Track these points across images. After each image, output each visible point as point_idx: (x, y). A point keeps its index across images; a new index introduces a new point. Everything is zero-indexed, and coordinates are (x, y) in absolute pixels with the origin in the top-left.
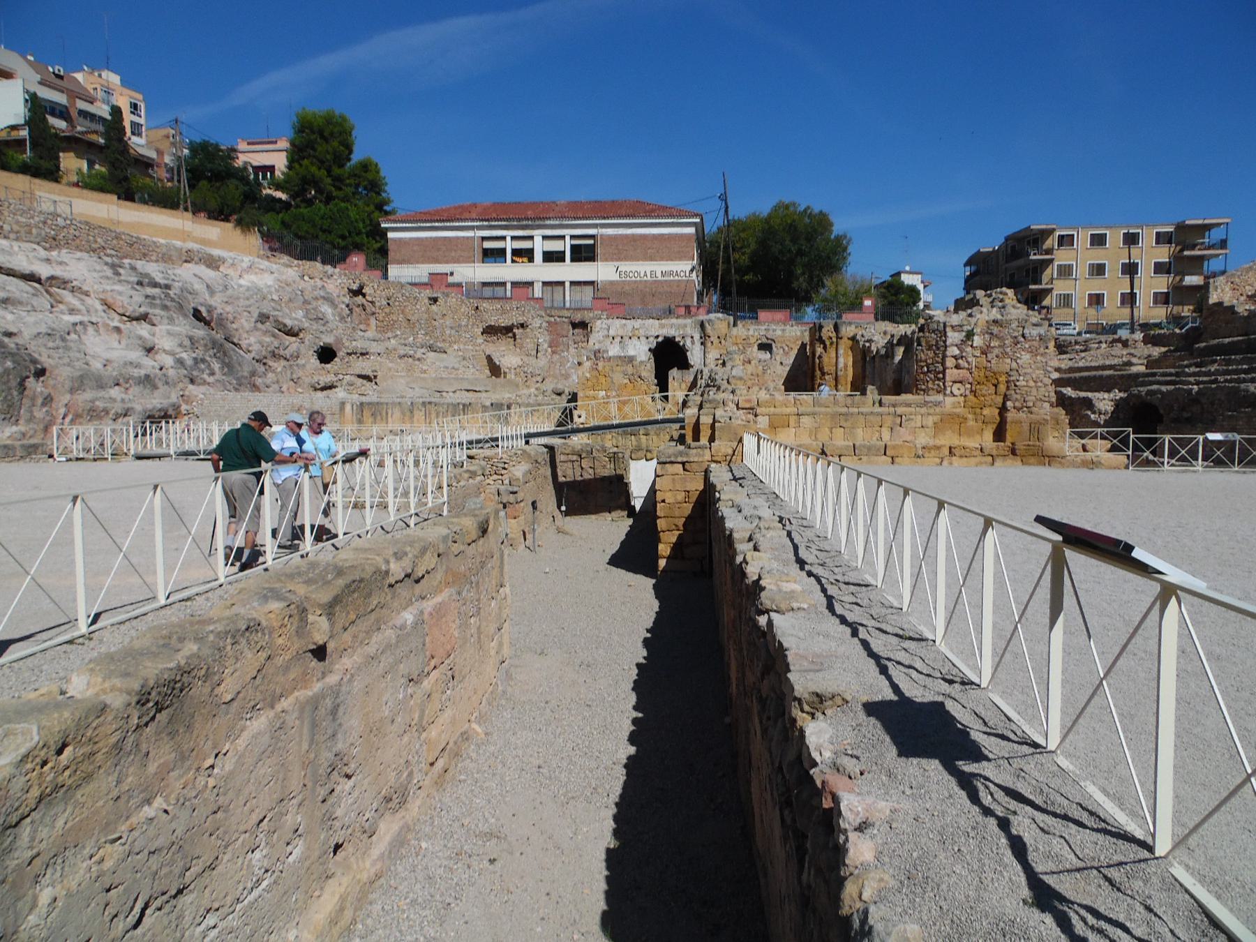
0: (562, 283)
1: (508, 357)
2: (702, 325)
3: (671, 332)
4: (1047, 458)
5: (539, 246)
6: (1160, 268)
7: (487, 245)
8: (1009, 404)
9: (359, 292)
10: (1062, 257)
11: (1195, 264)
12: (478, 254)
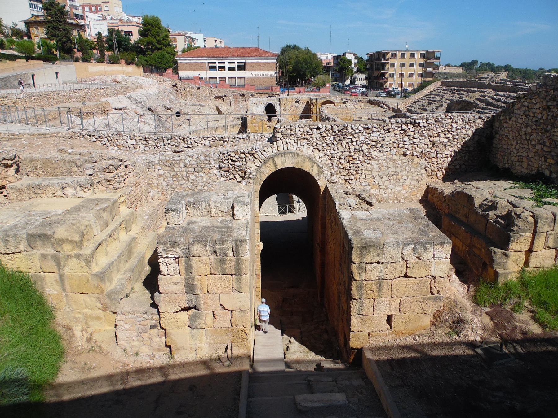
0: (235, 78)
1: (224, 108)
2: (279, 100)
3: (270, 102)
5: (227, 66)
6: (421, 65)
7: (210, 65)
9: (175, 86)
10: (391, 61)
11: (431, 65)
12: (208, 68)
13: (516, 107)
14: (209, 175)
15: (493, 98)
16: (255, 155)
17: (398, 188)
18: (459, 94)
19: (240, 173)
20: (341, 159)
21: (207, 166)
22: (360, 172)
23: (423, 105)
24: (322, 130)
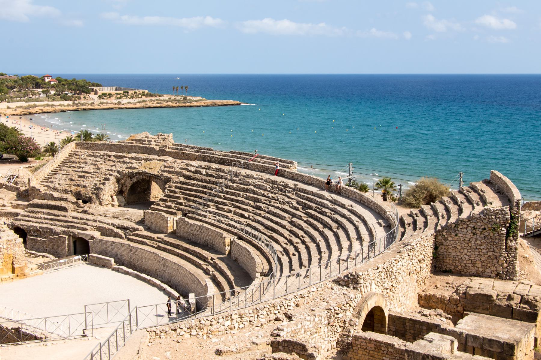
4: (24, 276)
8: (14, 263)
13: (461, 227)
14: (320, 334)
15: (187, 170)
16: (351, 304)
17: (408, 302)
18: (124, 162)
19: (340, 324)
20: (387, 289)
21: (320, 326)
22: (395, 297)
23: (71, 180)
24: (380, 269)
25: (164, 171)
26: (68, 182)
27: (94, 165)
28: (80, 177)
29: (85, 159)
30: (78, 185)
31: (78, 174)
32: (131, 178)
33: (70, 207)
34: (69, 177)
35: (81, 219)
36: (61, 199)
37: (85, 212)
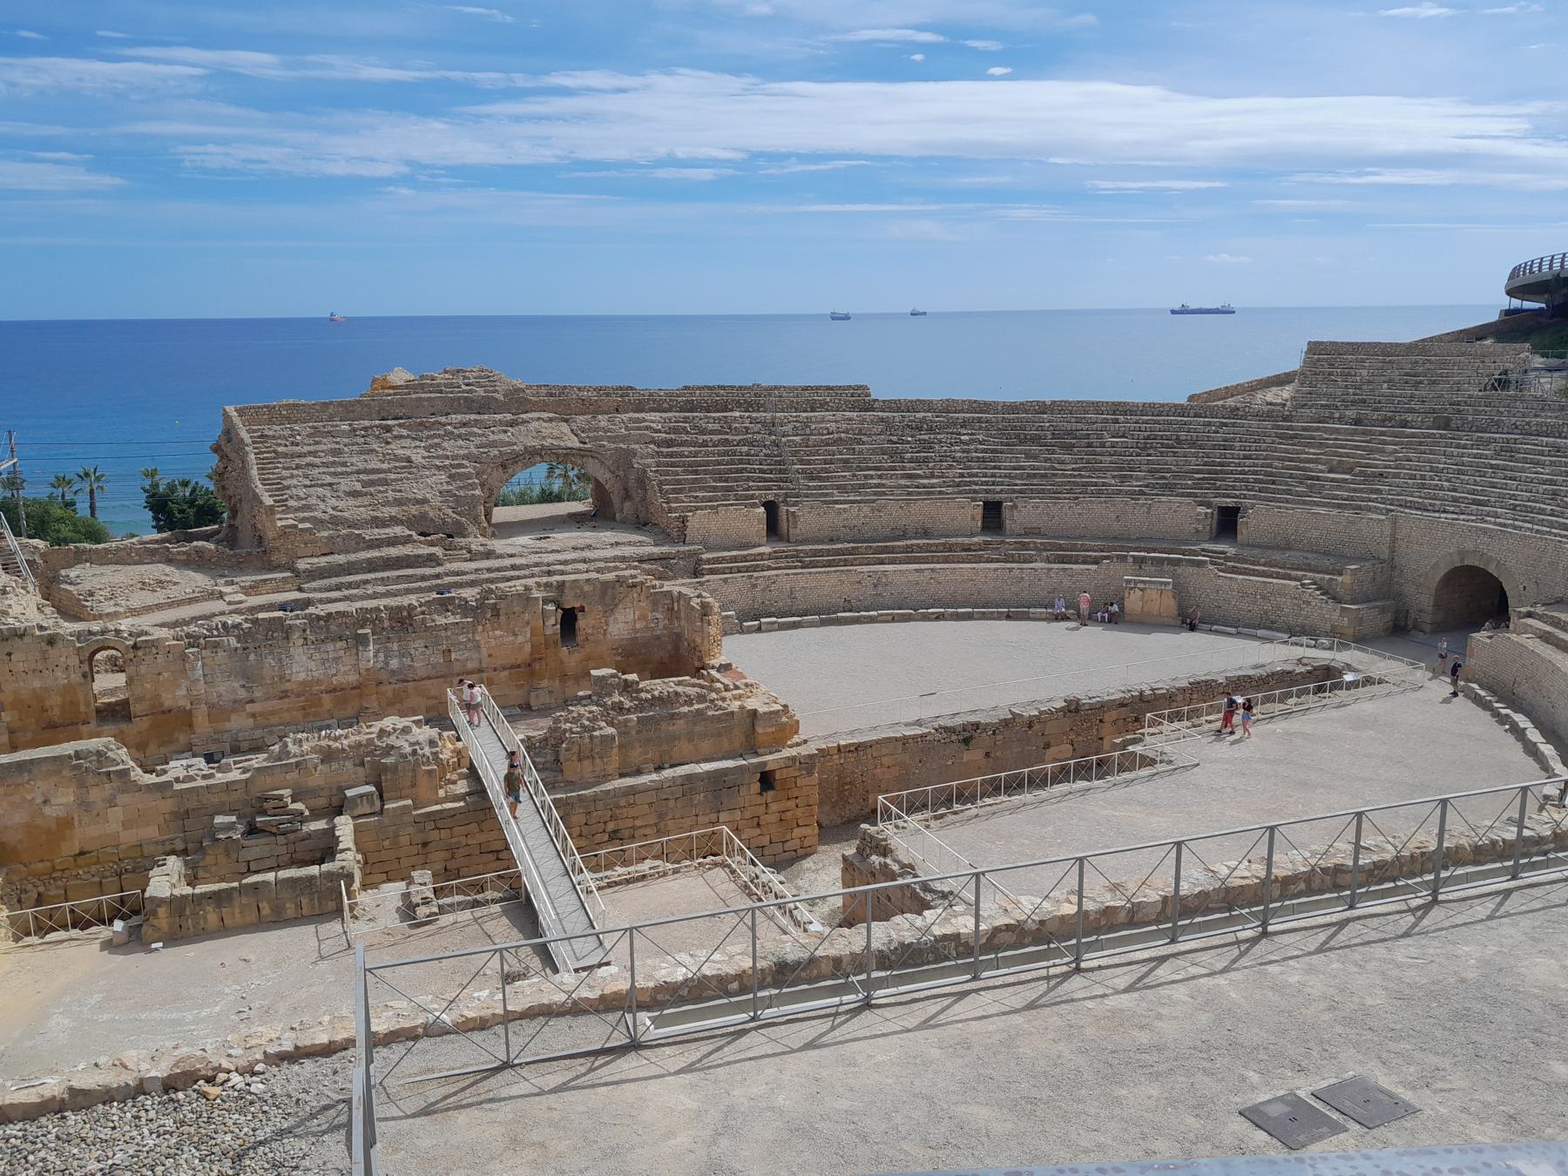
25: (596, 439)
26: (351, 502)
27: (361, 453)
28: (372, 483)
29: (317, 443)
30: (399, 502)
31: (354, 477)
32: (504, 466)
33: (438, 551)
34: (343, 487)
35: (514, 567)
36: (393, 542)
37: (489, 555)
